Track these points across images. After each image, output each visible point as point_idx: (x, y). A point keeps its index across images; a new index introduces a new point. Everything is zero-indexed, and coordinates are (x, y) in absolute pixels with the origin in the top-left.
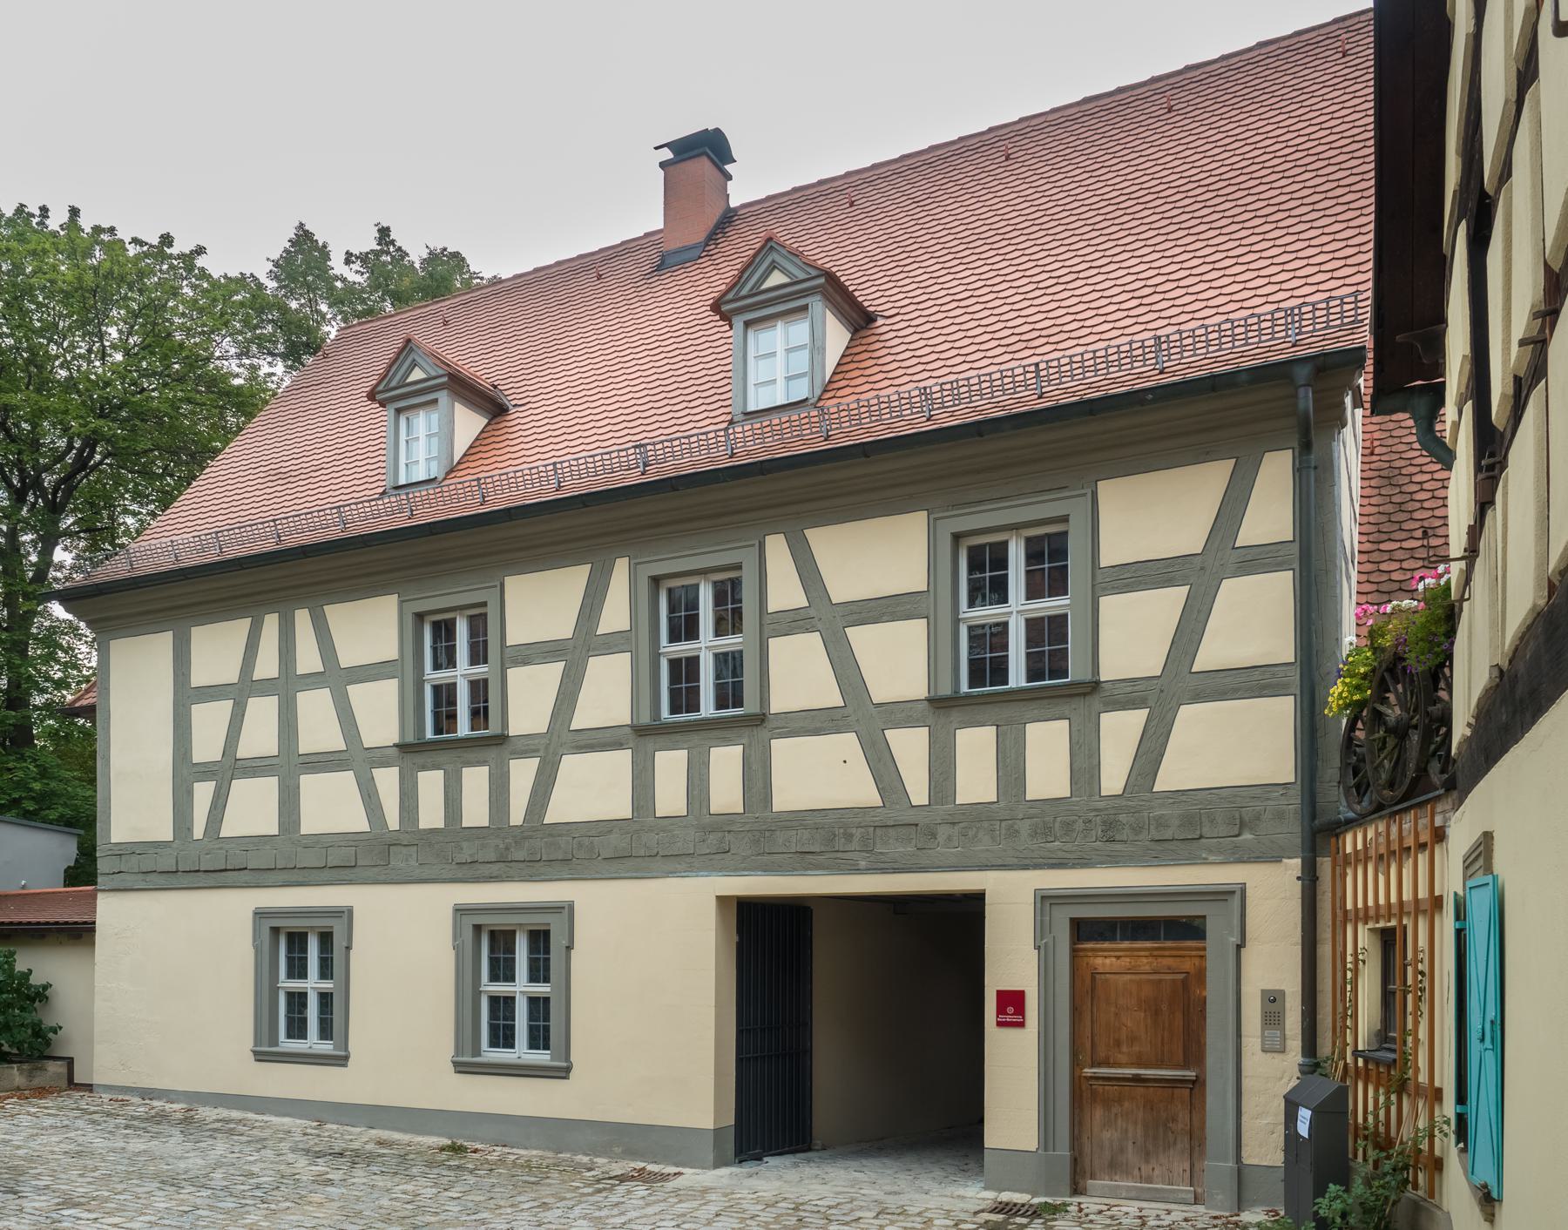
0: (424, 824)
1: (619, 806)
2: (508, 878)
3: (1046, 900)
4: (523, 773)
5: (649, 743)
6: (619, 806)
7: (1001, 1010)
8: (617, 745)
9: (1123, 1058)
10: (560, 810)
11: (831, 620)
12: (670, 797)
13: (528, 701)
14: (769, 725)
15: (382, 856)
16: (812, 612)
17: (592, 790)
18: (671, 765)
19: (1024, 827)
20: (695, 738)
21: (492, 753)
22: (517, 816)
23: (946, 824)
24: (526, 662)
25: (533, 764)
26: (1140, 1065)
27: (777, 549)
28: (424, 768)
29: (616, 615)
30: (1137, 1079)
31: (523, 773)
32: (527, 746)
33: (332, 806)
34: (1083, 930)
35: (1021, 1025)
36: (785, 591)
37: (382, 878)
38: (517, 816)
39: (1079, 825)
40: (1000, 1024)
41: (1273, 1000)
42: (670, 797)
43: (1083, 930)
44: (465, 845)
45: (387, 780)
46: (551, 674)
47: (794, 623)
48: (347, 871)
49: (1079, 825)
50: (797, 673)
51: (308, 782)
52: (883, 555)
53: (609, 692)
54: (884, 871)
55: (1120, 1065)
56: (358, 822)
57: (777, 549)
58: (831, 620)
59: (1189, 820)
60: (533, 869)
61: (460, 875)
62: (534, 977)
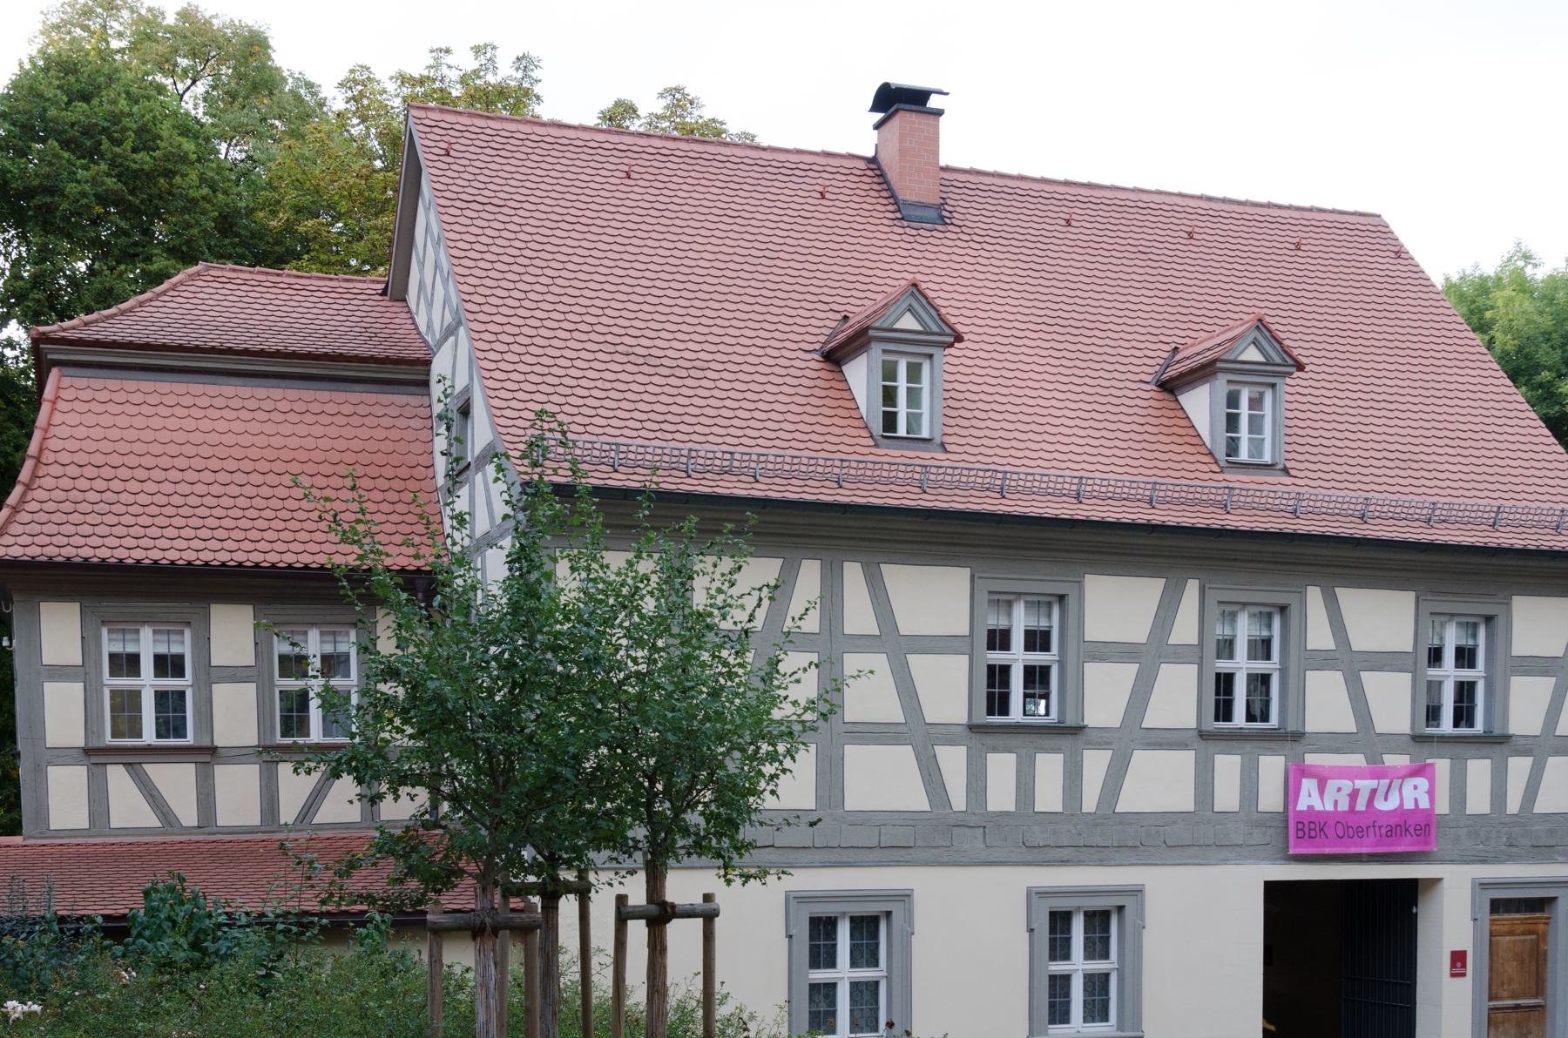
0: (992, 806)
1: (1184, 800)
2: (1080, 863)
3: (1484, 885)
4: (1096, 764)
5: (1211, 746)
6: (1184, 800)
7: (1453, 965)
8: (1181, 745)
9: (1505, 994)
10: (1131, 800)
11: (1352, 664)
12: (1227, 796)
13: (1103, 695)
14: (1304, 741)
15: (943, 836)
16: (1338, 655)
17: (1160, 784)
18: (1228, 765)
19: (1463, 833)
20: (1248, 746)
21: (1066, 742)
22: (1090, 803)
23: (1415, 832)
24: (1101, 658)
25: (1106, 755)
26: (1513, 997)
27: (1314, 595)
28: (995, 750)
29: (1185, 629)
30: (1517, 1007)
31: (1096, 764)
32: (1102, 739)
33: (882, 781)
34: (1497, 906)
35: (1464, 975)
36: (1319, 636)
37: (945, 859)
38: (1090, 803)
39: (1494, 834)
40: (1453, 975)
41: (1458, 958)
42: (1227, 796)
43: (1497, 906)
44: (1036, 829)
45: (953, 760)
46: (1126, 673)
47: (1324, 661)
48: (902, 851)
49: (1494, 834)
50: (1324, 703)
51: (855, 754)
52: (1383, 618)
53: (1178, 698)
54: (1484, 862)
55: (1502, 999)
56: (919, 801)
57: (1314, 595)
58: (1352, 664)
59: (1551, 832)
60: (1101, 854)
61: (1029, 858)
62: (1090, 954)
